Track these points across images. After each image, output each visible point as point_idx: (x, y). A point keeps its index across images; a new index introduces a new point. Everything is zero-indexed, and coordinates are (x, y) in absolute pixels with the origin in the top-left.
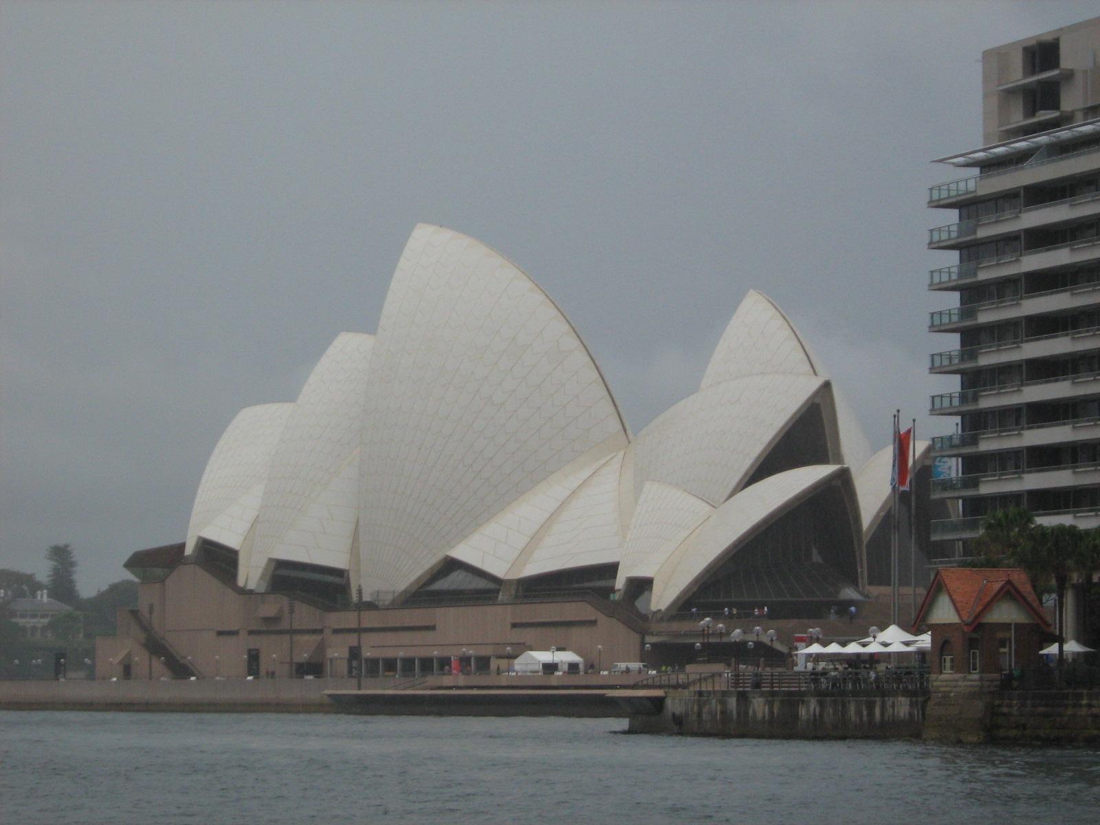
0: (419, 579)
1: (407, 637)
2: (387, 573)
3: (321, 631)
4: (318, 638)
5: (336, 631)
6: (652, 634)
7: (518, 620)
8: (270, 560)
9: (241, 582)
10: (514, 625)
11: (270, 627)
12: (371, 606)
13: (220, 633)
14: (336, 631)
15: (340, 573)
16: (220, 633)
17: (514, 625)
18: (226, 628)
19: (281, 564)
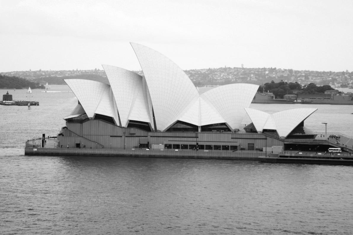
0: (171, 125)
1: (185, 139)
2: (164, 123)
3: (147, 136)
4: (147, 138)
5: (151, 137)
6: (287, 142)
7: (232, 137)
8: (129, 120)
9: (118, 125)
10: (232, 138)
11: (132, 135)
12: (160, 132)
13: (111, 136)
14: (151, 137)
15: (147, 123)
16: (111, 136)
17: (232, 138)
18: (115, 135)
19: (130, 121)
